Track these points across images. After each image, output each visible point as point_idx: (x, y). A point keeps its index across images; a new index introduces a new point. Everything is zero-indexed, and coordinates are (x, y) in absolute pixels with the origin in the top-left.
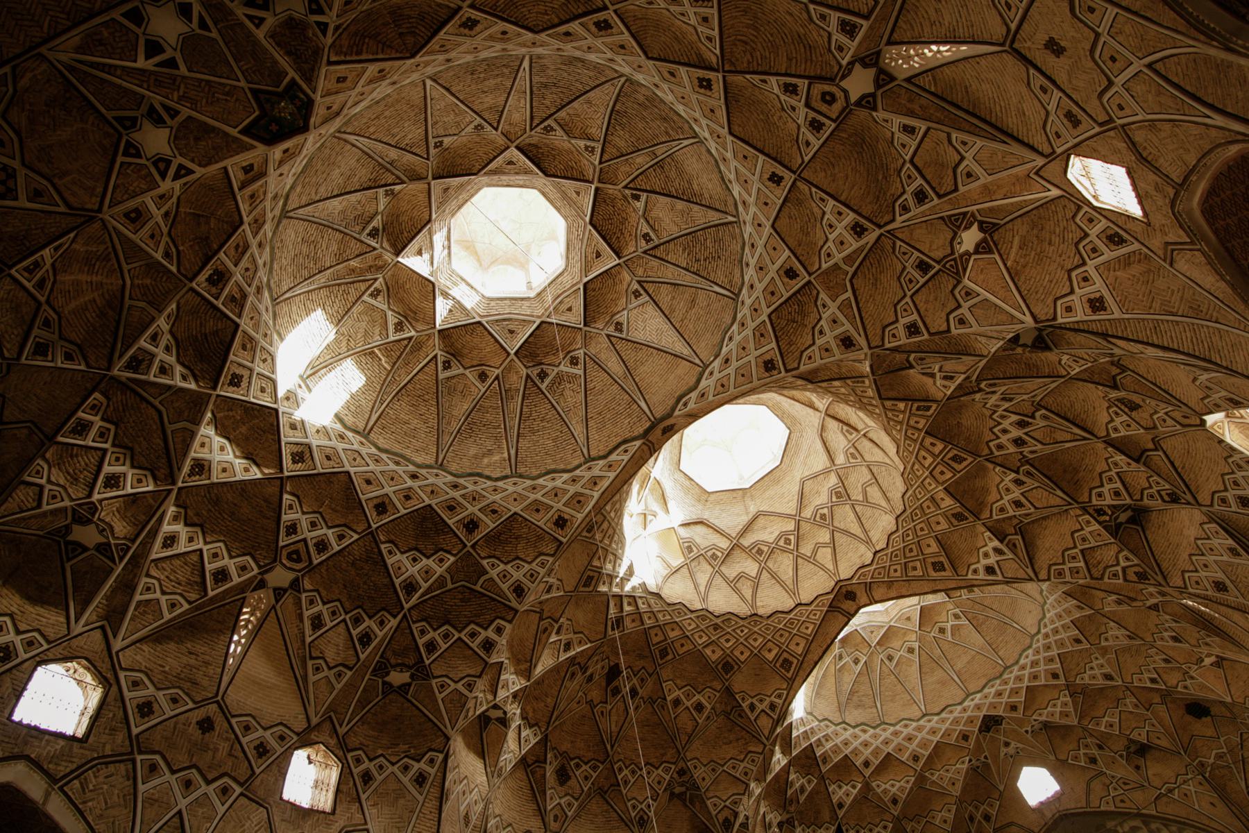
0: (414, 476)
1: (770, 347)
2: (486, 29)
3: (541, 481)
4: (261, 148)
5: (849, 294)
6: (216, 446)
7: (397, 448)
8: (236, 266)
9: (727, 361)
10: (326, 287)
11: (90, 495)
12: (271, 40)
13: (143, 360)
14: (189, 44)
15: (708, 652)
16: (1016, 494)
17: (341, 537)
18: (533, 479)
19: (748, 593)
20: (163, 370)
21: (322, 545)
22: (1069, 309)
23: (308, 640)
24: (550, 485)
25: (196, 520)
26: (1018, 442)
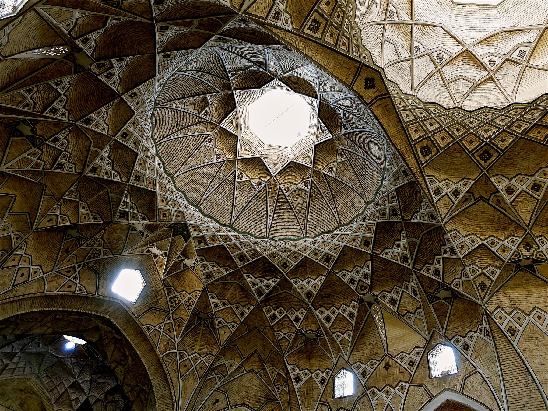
0: (364, 219)
2: (139, 172)
4: (191, 239)
6: (306, 285)
7: (352, 216)
8: (240, 250)
10: (275, 210)
11: (296, 328)
13: (260, 291)
17: (368, 267)
20: (268, 286)
21: (366, 276)
23: (395, 311)
25: (329, 306)
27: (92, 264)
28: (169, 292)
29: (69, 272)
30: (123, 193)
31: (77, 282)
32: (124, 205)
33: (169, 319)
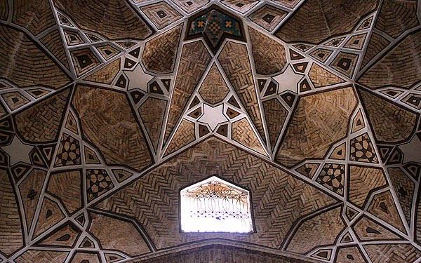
4: (246, 23)
12: (172, 68)
14: (212, 102)
27: (106, 205)
28: (307, 171)
29: (66, 238)
30: (53, 16)
31: (97, 249)
32: (73, 39)
33: (352, 213)
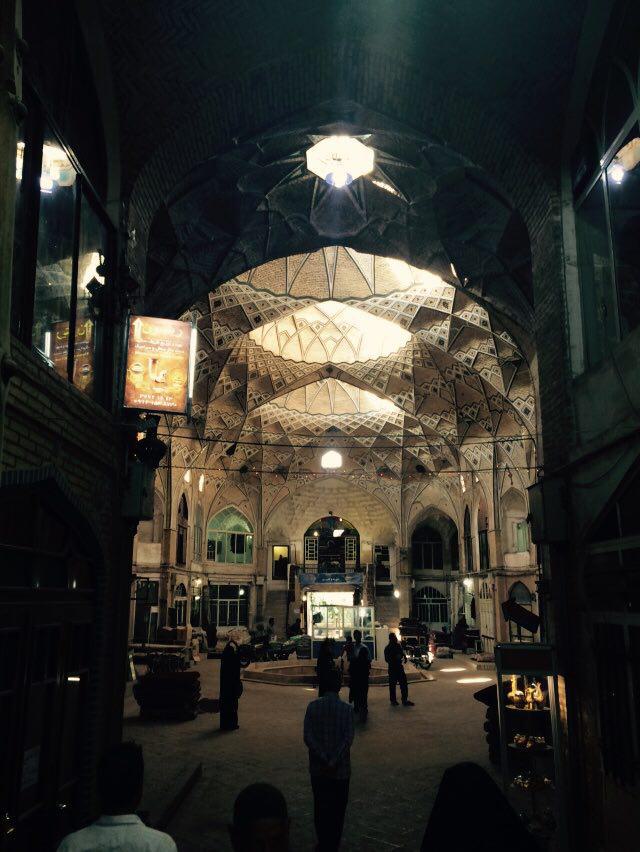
1: (412, 316)
3: (259, 293)
5: (459, 330)
9: (387, 303)
15: (250, 366)
16: (438, 387)
18: (257, 290)
19: (282, 343)
22: (519, 404)
24: (264, 298)
26: (458, 376)
